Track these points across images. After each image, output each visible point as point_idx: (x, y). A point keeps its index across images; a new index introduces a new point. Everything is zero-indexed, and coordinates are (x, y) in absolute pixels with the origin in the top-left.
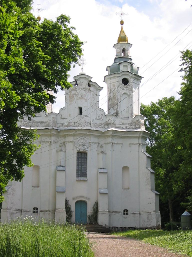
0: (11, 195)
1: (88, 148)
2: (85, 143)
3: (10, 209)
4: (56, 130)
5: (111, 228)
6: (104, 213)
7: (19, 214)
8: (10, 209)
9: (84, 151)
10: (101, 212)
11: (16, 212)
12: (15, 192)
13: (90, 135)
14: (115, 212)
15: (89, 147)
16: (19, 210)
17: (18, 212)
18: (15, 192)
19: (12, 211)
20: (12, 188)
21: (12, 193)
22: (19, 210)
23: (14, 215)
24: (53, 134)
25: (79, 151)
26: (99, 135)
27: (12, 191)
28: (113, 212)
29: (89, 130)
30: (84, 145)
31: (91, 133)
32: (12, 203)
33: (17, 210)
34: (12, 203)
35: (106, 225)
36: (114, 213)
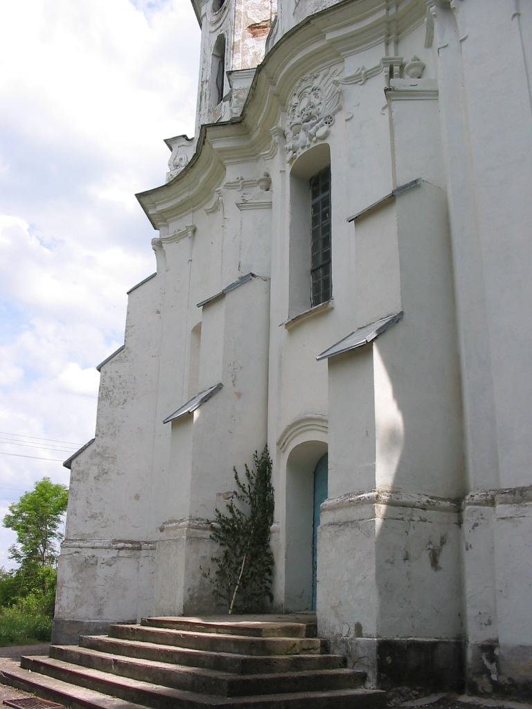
0: (91, 478)
1: (329, 121)
2: (317, 101)
3: (77, 544)
4: (227, 130)
5: (470, 654)
6: (346, 523)
7: (126, 567)
8: (77, 544)
9: (313, 145)
10: (339, 515)
11: (114, 553)
12: (113, 462)
13: (336, 52)
14: (512, 492)
15: (340, 109)
16: (130, 545)
17: (122, 553)
18: (113, 462)
19: (90, 553)
20: (98, 450)
21: (95, 471)
22: (127, 545)
23: (102, 571)
24: (220, 151)
25: (294, 161)
26: (388, 22)
27: (97, 460)
28: (492, 503)
29: (308, 31)
30: (310, 117)
31: (330, 36)
32: (93, 517)
33: (120, 545)
34: (93, 517)
35: (359, 629)
36: (502, 509)
